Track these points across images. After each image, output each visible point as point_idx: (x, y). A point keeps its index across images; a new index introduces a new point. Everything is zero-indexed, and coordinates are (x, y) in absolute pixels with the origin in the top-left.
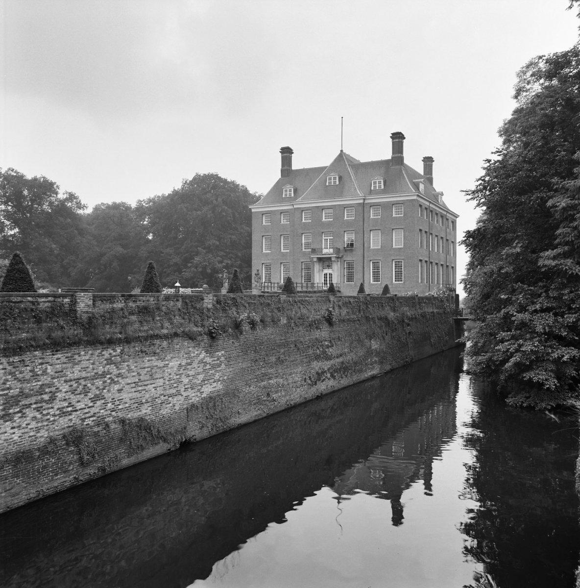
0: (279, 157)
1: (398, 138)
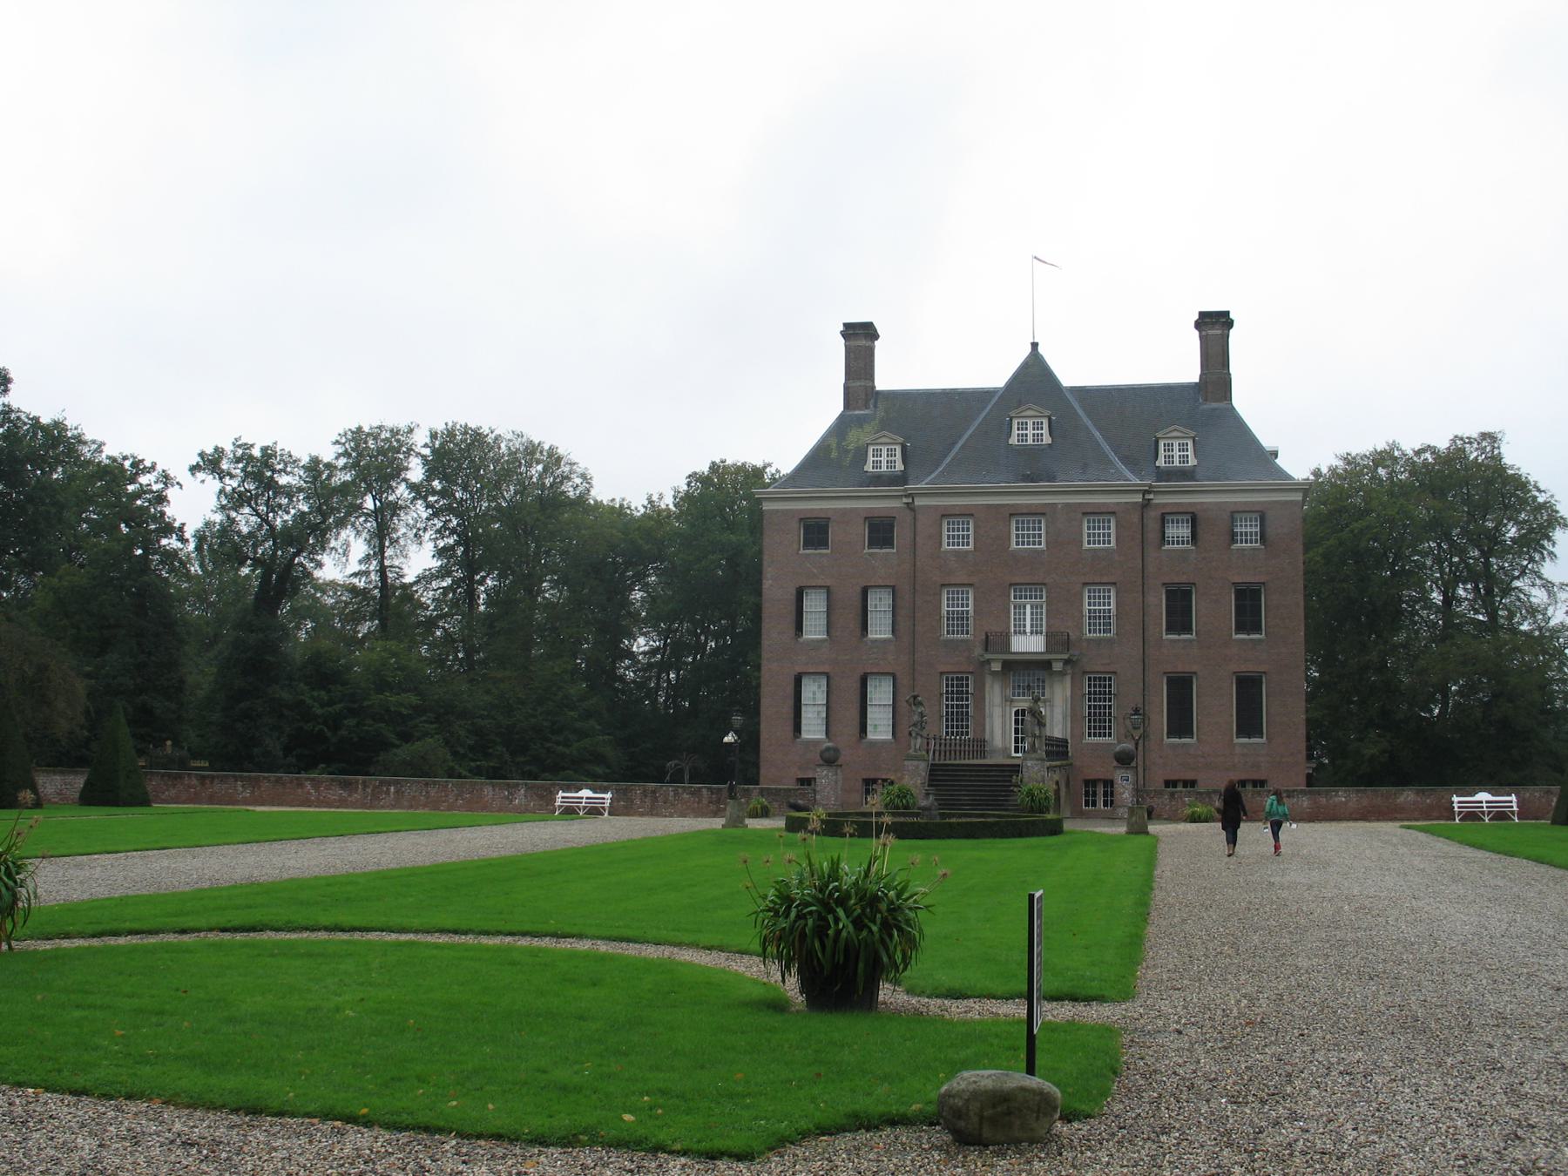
0: (837, 349)
1: (1215, 326)
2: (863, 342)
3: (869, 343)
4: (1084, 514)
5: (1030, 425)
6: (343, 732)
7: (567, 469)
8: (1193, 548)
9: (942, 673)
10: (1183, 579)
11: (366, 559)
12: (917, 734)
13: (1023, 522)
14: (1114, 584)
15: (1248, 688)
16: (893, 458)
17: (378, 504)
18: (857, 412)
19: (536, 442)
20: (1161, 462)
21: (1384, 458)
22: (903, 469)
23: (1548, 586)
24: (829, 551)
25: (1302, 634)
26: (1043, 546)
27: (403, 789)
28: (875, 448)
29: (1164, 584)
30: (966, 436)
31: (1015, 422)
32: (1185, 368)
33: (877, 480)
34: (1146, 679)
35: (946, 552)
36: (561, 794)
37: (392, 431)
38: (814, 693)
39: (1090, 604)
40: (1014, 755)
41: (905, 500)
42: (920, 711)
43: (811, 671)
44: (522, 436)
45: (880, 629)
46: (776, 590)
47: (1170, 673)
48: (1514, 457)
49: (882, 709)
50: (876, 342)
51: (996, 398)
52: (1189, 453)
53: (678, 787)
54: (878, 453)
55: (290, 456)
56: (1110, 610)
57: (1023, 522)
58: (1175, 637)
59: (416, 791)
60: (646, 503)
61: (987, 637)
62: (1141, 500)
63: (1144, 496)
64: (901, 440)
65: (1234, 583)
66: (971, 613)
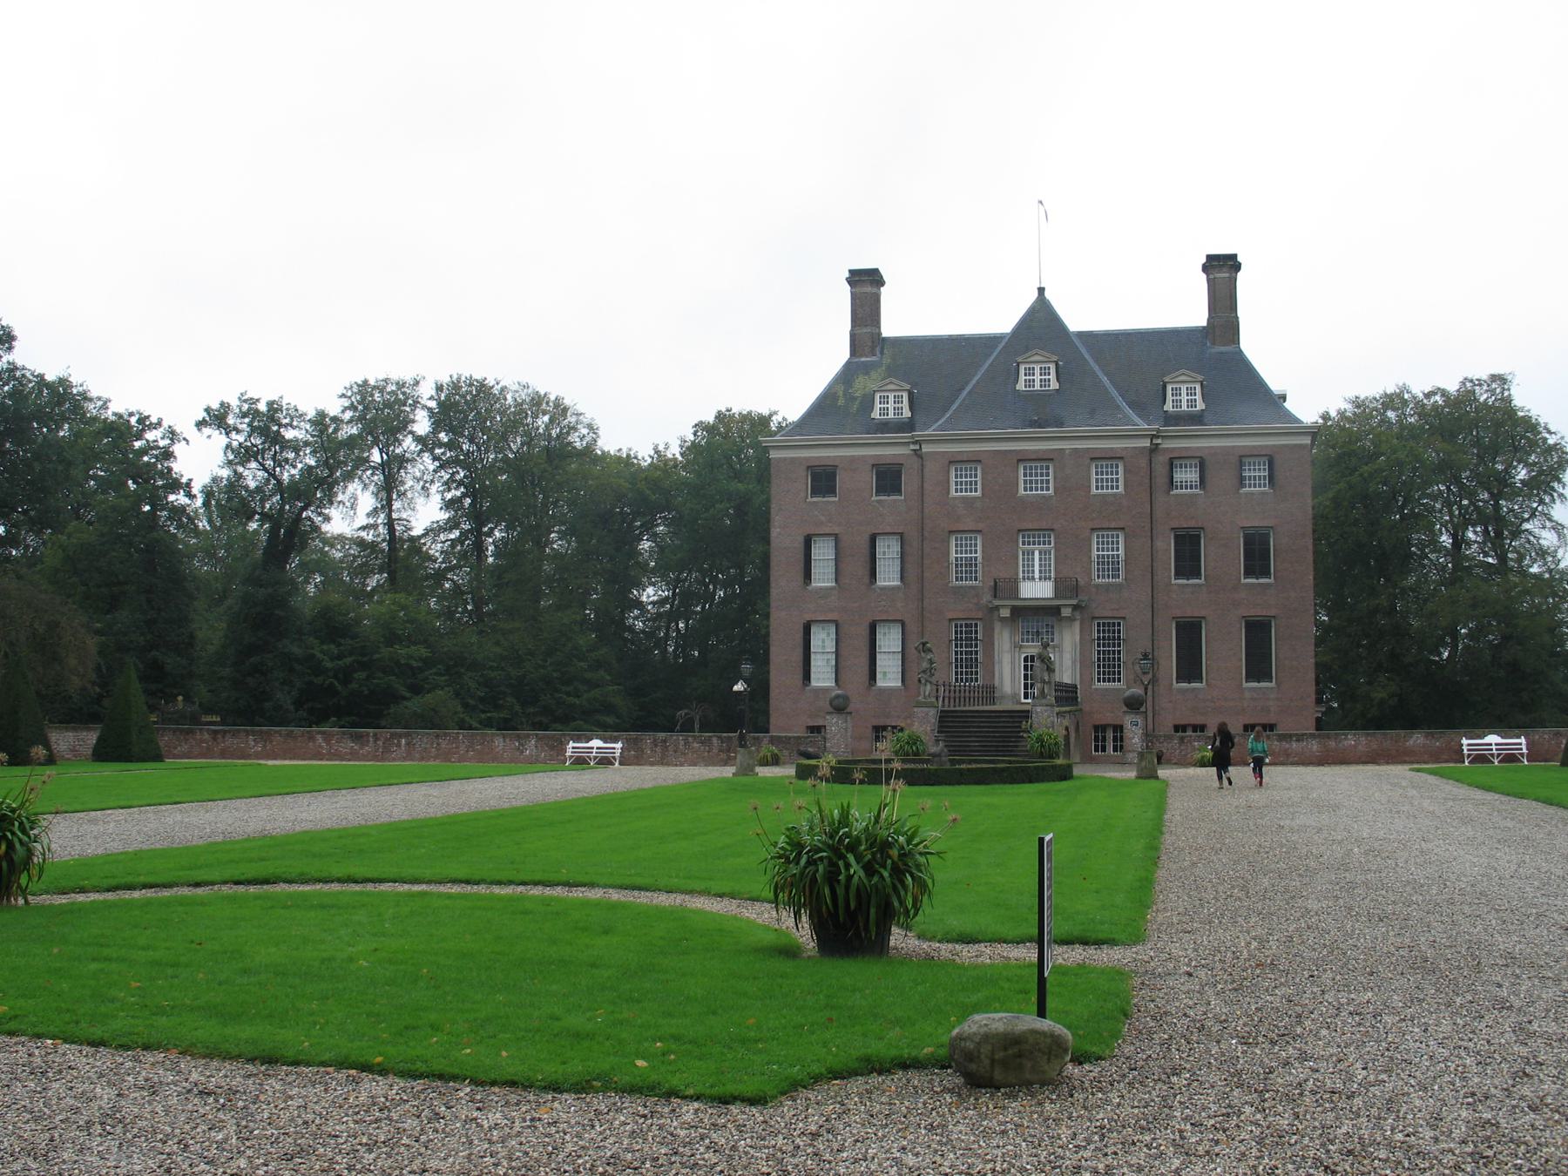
1: (1221, 269)
2: (869, 289)
3: (874, 290)
4: (1092, 459)
5: (1037, 371)
6: (354, 686)
7: (573, 419)
8: (1202, 492)
9: (950, 620)
10: (1192, 524)
11: (375, 512)
12: (927, 681)
13: (1031, 468)
14: (1123, 529)
15: (1258, 632)
16: (900, 405)
17: (385, 457)
18: (863, 359)
19: (542, 393)
20: (1169, 407)
21: (1393, 400)
22: (910, 416)
23: (1558, 528)
24: (837, 499)
25: (1311, 577)
26: (1051, 491)
27: (414, 741)
28: (882, 394)
29: (1173, 529)
30: (974, 382)
31: (1022, 368)
32: (1193, 312)
33: (885, 426)
34: (1155, 623)
35: (955, 498)
36: (571, 744)
37: (397, 383)
38: (823, 641)
39: (1098, 550)
40: (1023, 700)
41: (912, 447)
42: (929, 657)
44: (528, 387)
45: (888, 576)
46: (783, 537)
47: (1177, 618)
48: (1525, 399)
49: (891, 656)
50: (882, 289)
51: (1003, 344)
52: (1197, 397)
53: (689, 736)
54: (885, 400)
55: (296, 410)
56: (1118, 555)
57: (1031, 468)
58: (1185, 582)
59: (427, 743)
60: (652, 453)
61: (996, 583)
62: (1149, 445)
63: (1152, 441)
64: (908, 387)
65: (1242, 528)
66: (980, 559)
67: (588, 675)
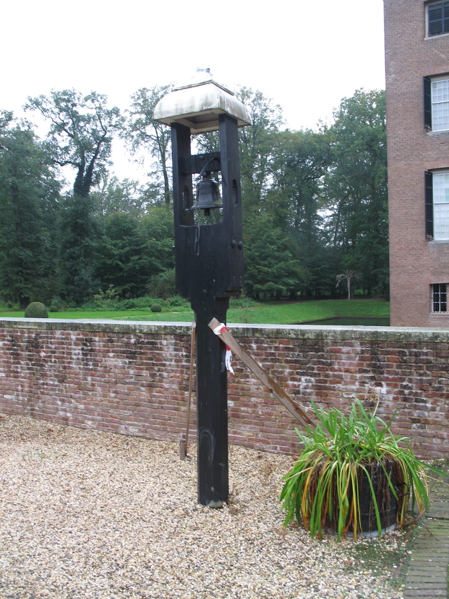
6: (131, 264)
43: (443, 167)
67: (277, 254)
